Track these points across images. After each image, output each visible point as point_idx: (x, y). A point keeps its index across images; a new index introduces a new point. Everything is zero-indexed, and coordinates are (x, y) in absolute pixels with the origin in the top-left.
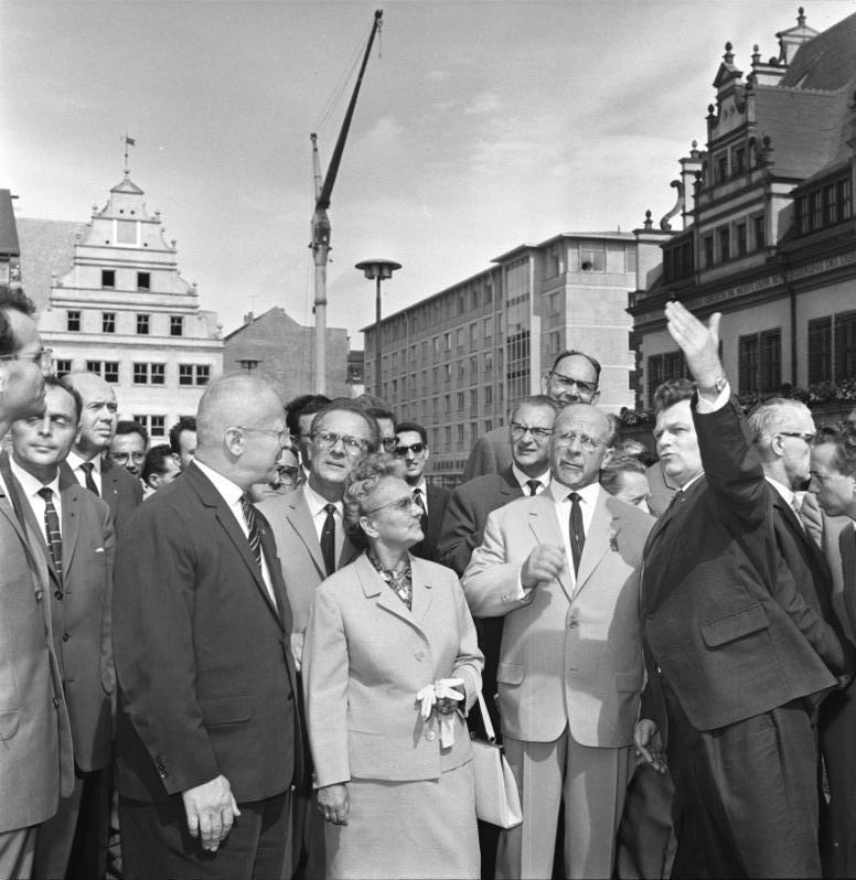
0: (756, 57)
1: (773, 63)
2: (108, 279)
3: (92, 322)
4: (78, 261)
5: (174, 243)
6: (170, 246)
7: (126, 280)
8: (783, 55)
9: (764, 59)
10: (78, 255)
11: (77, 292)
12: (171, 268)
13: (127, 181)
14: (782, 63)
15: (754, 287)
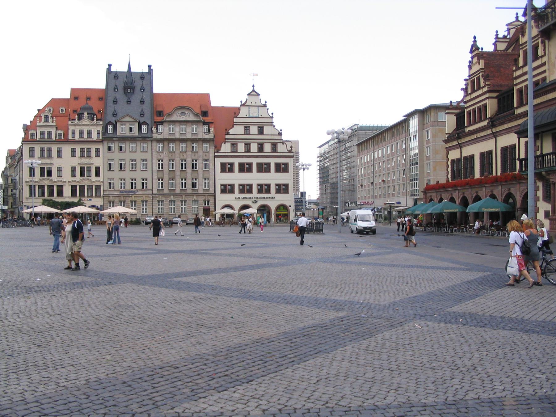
0: (497, 35)
1: (505, 37)
2: (247, 129)
3: (241, 147)
5: (272, 114)
7: (254, 130)
8: (509, 33)
9: (500, 36)
12: (271, 124)
13: (254, 90)
14: (508, 37)
15: (484, 133)
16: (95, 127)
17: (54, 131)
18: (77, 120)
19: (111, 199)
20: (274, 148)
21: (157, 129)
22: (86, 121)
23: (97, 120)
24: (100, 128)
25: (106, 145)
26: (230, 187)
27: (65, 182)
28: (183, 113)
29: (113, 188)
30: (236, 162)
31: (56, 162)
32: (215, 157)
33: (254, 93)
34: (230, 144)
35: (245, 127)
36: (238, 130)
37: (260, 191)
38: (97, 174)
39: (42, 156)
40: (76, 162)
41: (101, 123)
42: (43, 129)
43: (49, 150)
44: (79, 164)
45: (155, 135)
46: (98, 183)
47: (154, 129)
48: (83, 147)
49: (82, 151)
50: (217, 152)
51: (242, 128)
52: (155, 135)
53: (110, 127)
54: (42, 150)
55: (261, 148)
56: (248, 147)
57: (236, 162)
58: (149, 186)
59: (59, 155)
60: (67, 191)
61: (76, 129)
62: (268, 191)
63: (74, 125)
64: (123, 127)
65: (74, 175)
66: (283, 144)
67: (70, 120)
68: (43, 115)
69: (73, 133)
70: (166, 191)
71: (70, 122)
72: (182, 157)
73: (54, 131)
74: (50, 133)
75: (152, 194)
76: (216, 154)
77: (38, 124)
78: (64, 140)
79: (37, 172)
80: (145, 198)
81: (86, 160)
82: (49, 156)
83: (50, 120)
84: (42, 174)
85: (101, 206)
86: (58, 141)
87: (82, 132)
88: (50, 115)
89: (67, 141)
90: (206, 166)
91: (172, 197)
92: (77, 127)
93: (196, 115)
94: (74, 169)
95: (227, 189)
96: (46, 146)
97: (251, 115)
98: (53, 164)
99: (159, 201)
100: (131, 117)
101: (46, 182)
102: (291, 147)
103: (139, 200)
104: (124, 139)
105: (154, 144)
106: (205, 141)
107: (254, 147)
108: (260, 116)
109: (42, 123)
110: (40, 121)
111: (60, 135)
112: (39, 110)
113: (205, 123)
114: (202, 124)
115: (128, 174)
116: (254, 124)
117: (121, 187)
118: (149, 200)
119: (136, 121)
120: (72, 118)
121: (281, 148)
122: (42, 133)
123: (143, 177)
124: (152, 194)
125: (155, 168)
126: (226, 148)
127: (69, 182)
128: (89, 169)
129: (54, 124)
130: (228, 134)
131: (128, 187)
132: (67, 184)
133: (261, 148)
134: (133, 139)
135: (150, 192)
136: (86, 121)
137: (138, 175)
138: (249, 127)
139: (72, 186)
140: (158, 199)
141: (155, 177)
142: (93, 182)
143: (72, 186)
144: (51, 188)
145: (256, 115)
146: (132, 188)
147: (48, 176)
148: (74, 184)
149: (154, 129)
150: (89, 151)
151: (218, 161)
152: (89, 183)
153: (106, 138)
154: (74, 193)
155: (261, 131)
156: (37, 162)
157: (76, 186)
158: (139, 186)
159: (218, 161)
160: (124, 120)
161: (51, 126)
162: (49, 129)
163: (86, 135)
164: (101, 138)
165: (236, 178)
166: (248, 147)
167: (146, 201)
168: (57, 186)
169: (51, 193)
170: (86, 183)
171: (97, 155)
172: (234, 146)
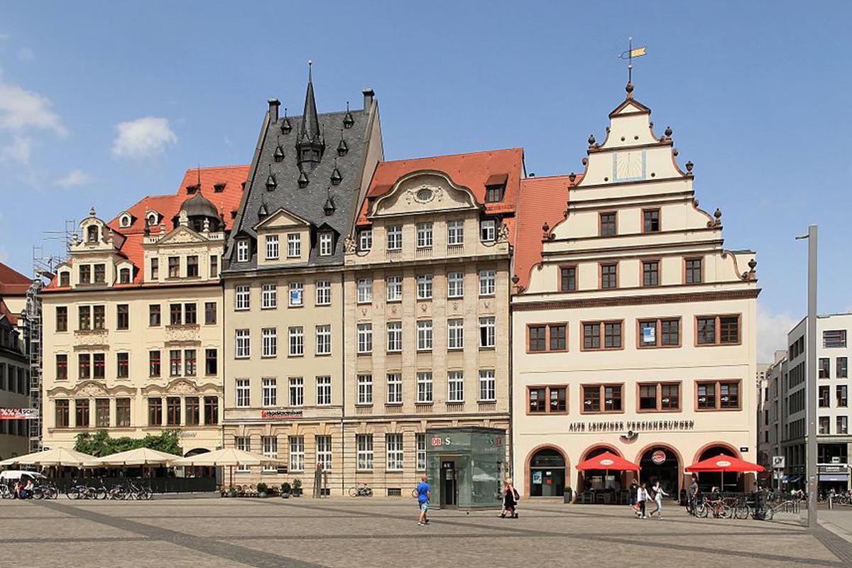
3: (589, 276)
10: (571, 200)
11: (572, 243)
16: (205, 248)
17: (109, 263)
19: (241, 432)
21: (358, 243)
22: (184, 236)
24: (218, 251)
25: (230, 293)
26: (555, 395)
27: (135, 390)
28: (424, 194)
29: (247, 402)
31: (114, 341)
32: (512, 308)
34: (555, 268)
38: (212, 368)
39: (83, 329)
40: (160, 337)
42: (85, 261)
43: (100, 310)
44: (167, 344)
46: (211, 392)
48: (175, 301)
49: (175, 308)
50: (518, 295)
51: (594, 217)
52: (353, 260)
54: (84, 311)
56: (609, 272)
58: (336, 398)
59: (123, 322)
60: (139, 412)
63: (156, 246)
65: (156, 371)
66: (724, 256)
69: (154, 268)
70: (379, 409)
72: (420, 313)
73: (109, 263)
74: (100, 269)
76: (515, 300)
78: (131, 286)
80: (322, 430)
81: (183, 334)
82: (100, 329)
83: (100, 236)
84: (84, 372)
87: (174, 263)
89: (142, 289)
91: (394, 424)
92: (161, 251)
93: (461, 193)
94: (155, 356)
98: (106, 347)
99: (360, 438)
100: (289, 215)
101: (91, 393)
103: (309, 434)
104: (271, 277)
106: (484, 265)
107: (630, 273)
109: (82, 247)
115: (283, 367)
117: (267, 402)
119: (301, 226)
121: (717, 269)
122: (84, 270)
123: (320, 375)
125: (352, 347)
128: (191, 356)
129: (110, 246)
131: (283, 400)
134: (294, 276)
135: (338, 412)
137: (309, 367)
139: (151, 400)
140: (357, 430)
141: (351, 373)
142: (197, 389)
143: (151, 400)
144: (102, 403)
147: (96, 375)
148: (154, 394)
149: (351, 245)
150: (191, 308)
151: (523, 319)
152: (191, 392)
153: (232, 277)
154: (155, 419)
158: (310, 396)
160: (273, 224)
161: (104, 254)
162: (99, 261)
163: (183, 271)
166: (609, 272)
167: (329, 438)
168: (168, 399)
170: (182, 391)
171: (211, 319)
172: (568, 276)
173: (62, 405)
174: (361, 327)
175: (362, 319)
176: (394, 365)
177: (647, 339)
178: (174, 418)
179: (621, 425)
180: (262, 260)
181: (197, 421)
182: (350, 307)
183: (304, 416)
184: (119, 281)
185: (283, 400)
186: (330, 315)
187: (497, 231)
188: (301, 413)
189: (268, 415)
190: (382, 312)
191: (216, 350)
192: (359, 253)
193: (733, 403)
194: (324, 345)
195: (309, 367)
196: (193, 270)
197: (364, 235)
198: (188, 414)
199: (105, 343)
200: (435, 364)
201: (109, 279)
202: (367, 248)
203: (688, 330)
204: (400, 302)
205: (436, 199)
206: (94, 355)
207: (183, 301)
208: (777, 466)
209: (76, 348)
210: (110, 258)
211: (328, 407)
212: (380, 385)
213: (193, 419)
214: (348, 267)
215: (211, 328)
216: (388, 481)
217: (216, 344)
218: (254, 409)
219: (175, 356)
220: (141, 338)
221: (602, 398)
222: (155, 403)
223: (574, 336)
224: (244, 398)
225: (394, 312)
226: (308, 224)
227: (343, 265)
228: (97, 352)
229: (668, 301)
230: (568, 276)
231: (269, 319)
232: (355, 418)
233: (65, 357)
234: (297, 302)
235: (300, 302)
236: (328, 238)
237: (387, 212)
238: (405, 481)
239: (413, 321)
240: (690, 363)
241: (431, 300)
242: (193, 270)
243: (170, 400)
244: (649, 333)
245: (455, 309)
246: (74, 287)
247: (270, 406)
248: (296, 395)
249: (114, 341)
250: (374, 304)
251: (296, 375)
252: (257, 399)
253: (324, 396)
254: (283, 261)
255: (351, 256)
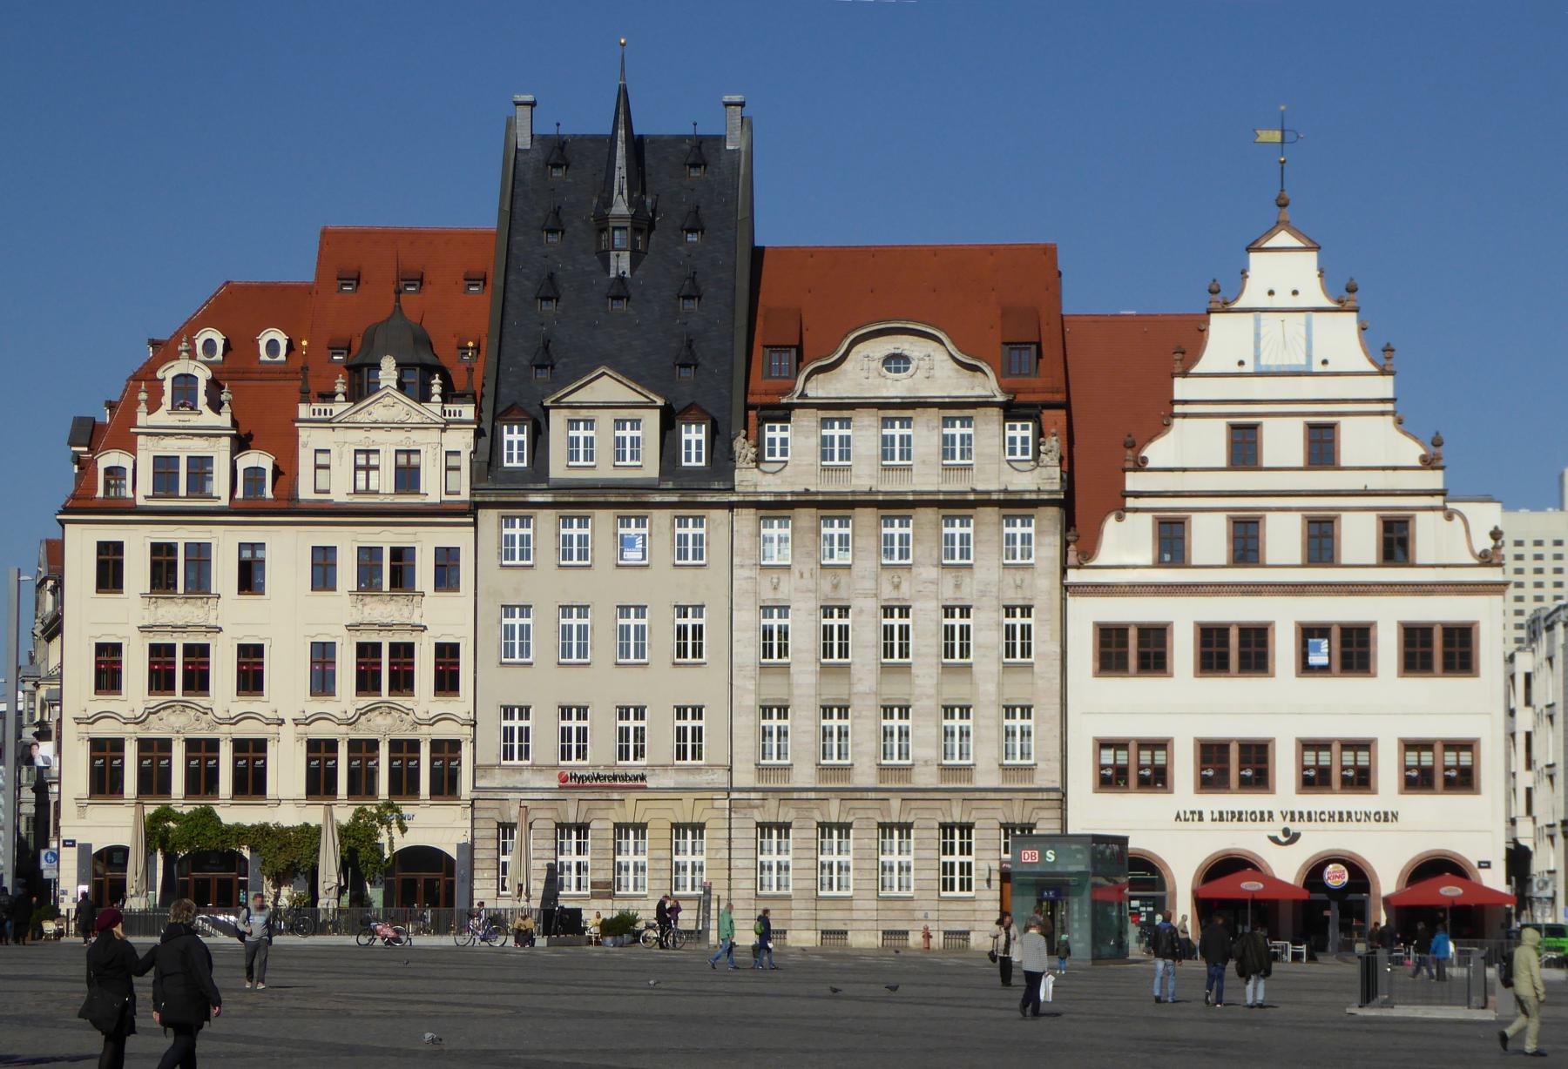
3: (1209, 538)
4: (1178, 409)
6: (1382, 361)
7: (1283, 441)
16: (434, 435)
18: (340, 398)
20: (1396, 542)
21: (759, 445)
22: (389, 404)
23: (447, 397)
24: (462, 440)
28: (896, 362)
30: (1183, 619)
31: (229, 619)
32: (1067, 589)
33: (1283, 238)
35: (1233, 427)
36: (1187, 449)
37: (1315, 780)
38: (447, 682)
41: (468, 412)
42: (169, 447)
44: (352, 627)
45: (748, 479)
46: (445, 731)
47: (743, 448)
49: (368, 557)
53: (515, 436)
55: (1321, 540)
57: (1183, 619)
58: (713, 748)
59: (250, 577)
60: (286, 769)
61: (340, 448)
62: (1361, 780)
63: (328, 422)
64: (582, 433)
65: (322, 682)
66: (1449, 517)
67: (306, 397)
68: (167, 374)
70: (804, 775)
71: (304, 411)
73: (220, 451)
74: (200, 468)
75: (730, 789)
76: (1074, 576)
77: (143, 418)
79: (135, 668)
81: (385, 609)
83: (202, 399)
84: (160, 680)
85: (460, 847)
86: (247, 509)
87: (365, 462)
88: (203, 375)
89: (289, 508)
90: (1017, 643)
92: (340, 435)
94: (323, 655)
95: (1134, 768)
96: (181, 535)
97: (1269, 360)
101: (177, 723)
102: (1496, 535)
103: (659, 817)
104: (581, 499)
105: (745, 518)
106: (1014, 505)
107: (1283, 538)
108: (1317, 367)
109: (163, 417)
110: (153, 406)
111: (255, 474)
112: (154, 343)
113: (1012, 411)
114: (996, 414)
115: (603, 686)
116: (1283, 408)
117: (565, 754)
118: (712, 815)
119: (650, 406)
120: (316, 386)
122: (165, 468)
124: (730, 789)
125: (748, 650)
126: (1126, 543)
127: (296, 722)
128: (403, 652)
129: (224, 419)
130: (1140, 465)
132: (288, 731)
133: (1321, 540)
134: (628, 499)
135: (720, 778)
136: (389, 404)
137: (662, 685)
138: (1254, 427)
139: (314, 746)
141: (747, 700)
143: (314, 746)
144: (202, 749)
145: (1297, 360)
146: (623, 754)
147: (189, 687)
148: (322, 731)
155: (1322, 446)
156: (130, 619)
157: (332, 745)
158: (661, 744)
159: (1087, 614)
161: (211, 433)
162: (199, 447)
163: (384, 481)
164: (465, 495)
165: (1185, 707)
169: (202, 781)
173: (105, 753)
174: (767, 610)
175: (768, 596)
176: (835, 691)
177: (1315, 660)
178: (362, 783)
179: (1271, 814)
180: (558, 469)
181: (414, 790)
182: (746, 573)
183: (650, 783)
184: (240, 494)
185: (601, 753)
186: (705, 586)
187: (1037, 445)
188: (643, 778)
189: (573, 783)
190: (808, 582)
191: (458, 645)
192: (762, 466)
193: (1464, 780)
194: (689, 643)
195: (662, 685)
196: (407, 477)
197: (772, 429)
198: (352, 774)
199: (212, 622)
200: (917, 691)
201: (219, 486)
202: (778, 457)
203: (1387, 648)
204: (849, 567)
205: (920, 375)
206: (185, 646)
207: (386, 537)
208: (1541, 894)
209: (144, 629)
210: (226, 441)
211: (698, 768)
212: (803, 725)
213: (404, 783)
214: (745, 494)
215: (447, 598)
216: (822, 915)
217: (459, 633)
218: (538, 768)
219: (367, 652)
220: (293, 613)
221: (1235, 765)
222: (320, 750)
223: (1183, 649)
224: (516, 744)
225: (836, 587)
226: (660, 402)
227: (732, 490)
228: (192, 640)
229: (1351, 593)
230: (1171, 539)
231: (575, 587)
232: (755, 790)
233: (116, 648)
234: (633, 556)
235: (640, 555)
236: (699, 431)
237: (821, 393)
238: (855, 915)
239: (871, 606)
240: (1391, 708)
241: (909, 567)
242: (407, 477)
243: (354, 745)
244: (1318, 649)
245: (957, 586)
246: (140, 501)
247: (574, 761)
248: (630, 744)
249: (229, 619)
250: (796, 570)
251: (632, 701)
252: (545, 745)
253: (688, 745)
254: (604, 469)
255: (749, 472)
